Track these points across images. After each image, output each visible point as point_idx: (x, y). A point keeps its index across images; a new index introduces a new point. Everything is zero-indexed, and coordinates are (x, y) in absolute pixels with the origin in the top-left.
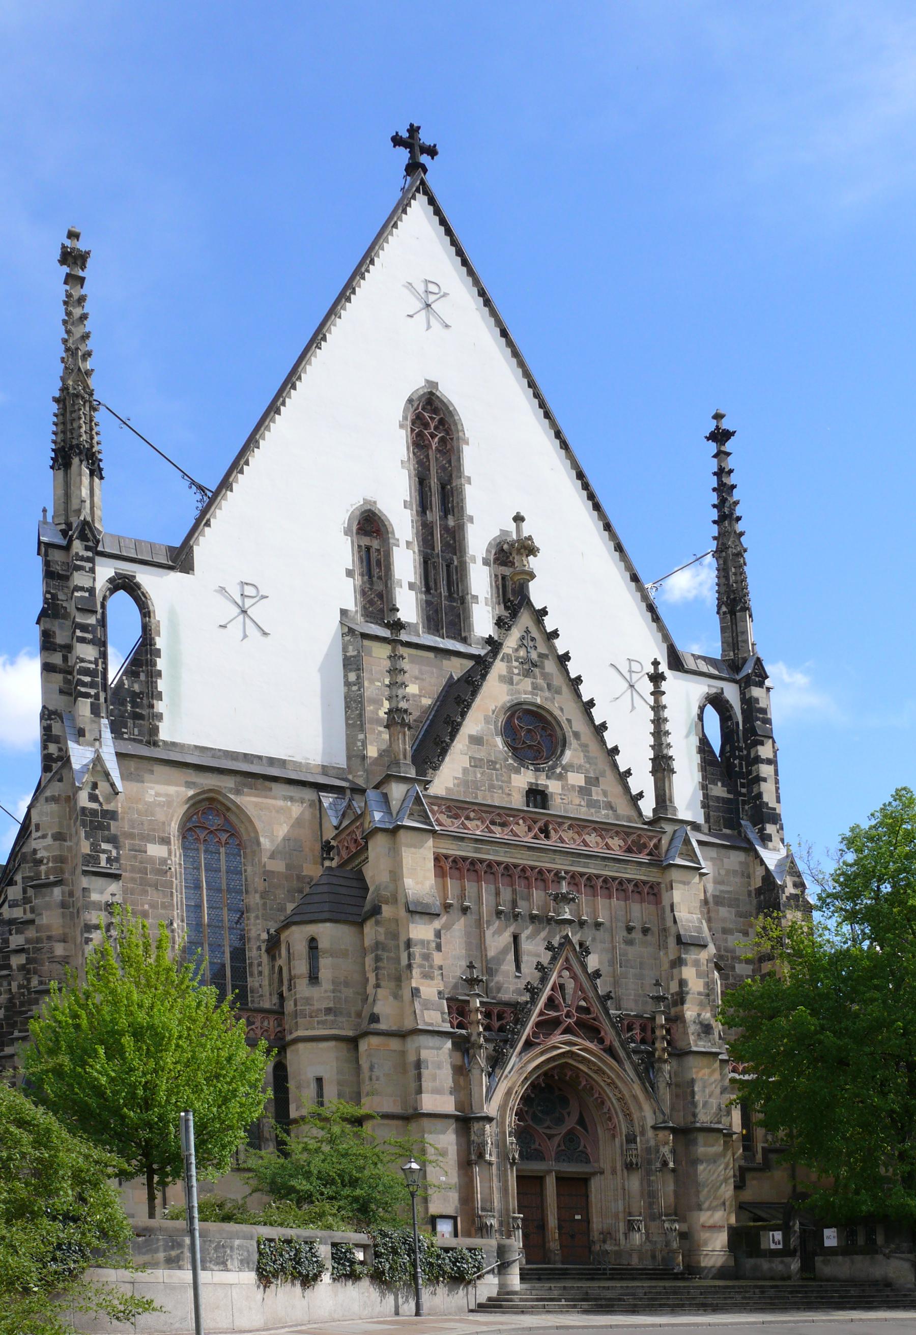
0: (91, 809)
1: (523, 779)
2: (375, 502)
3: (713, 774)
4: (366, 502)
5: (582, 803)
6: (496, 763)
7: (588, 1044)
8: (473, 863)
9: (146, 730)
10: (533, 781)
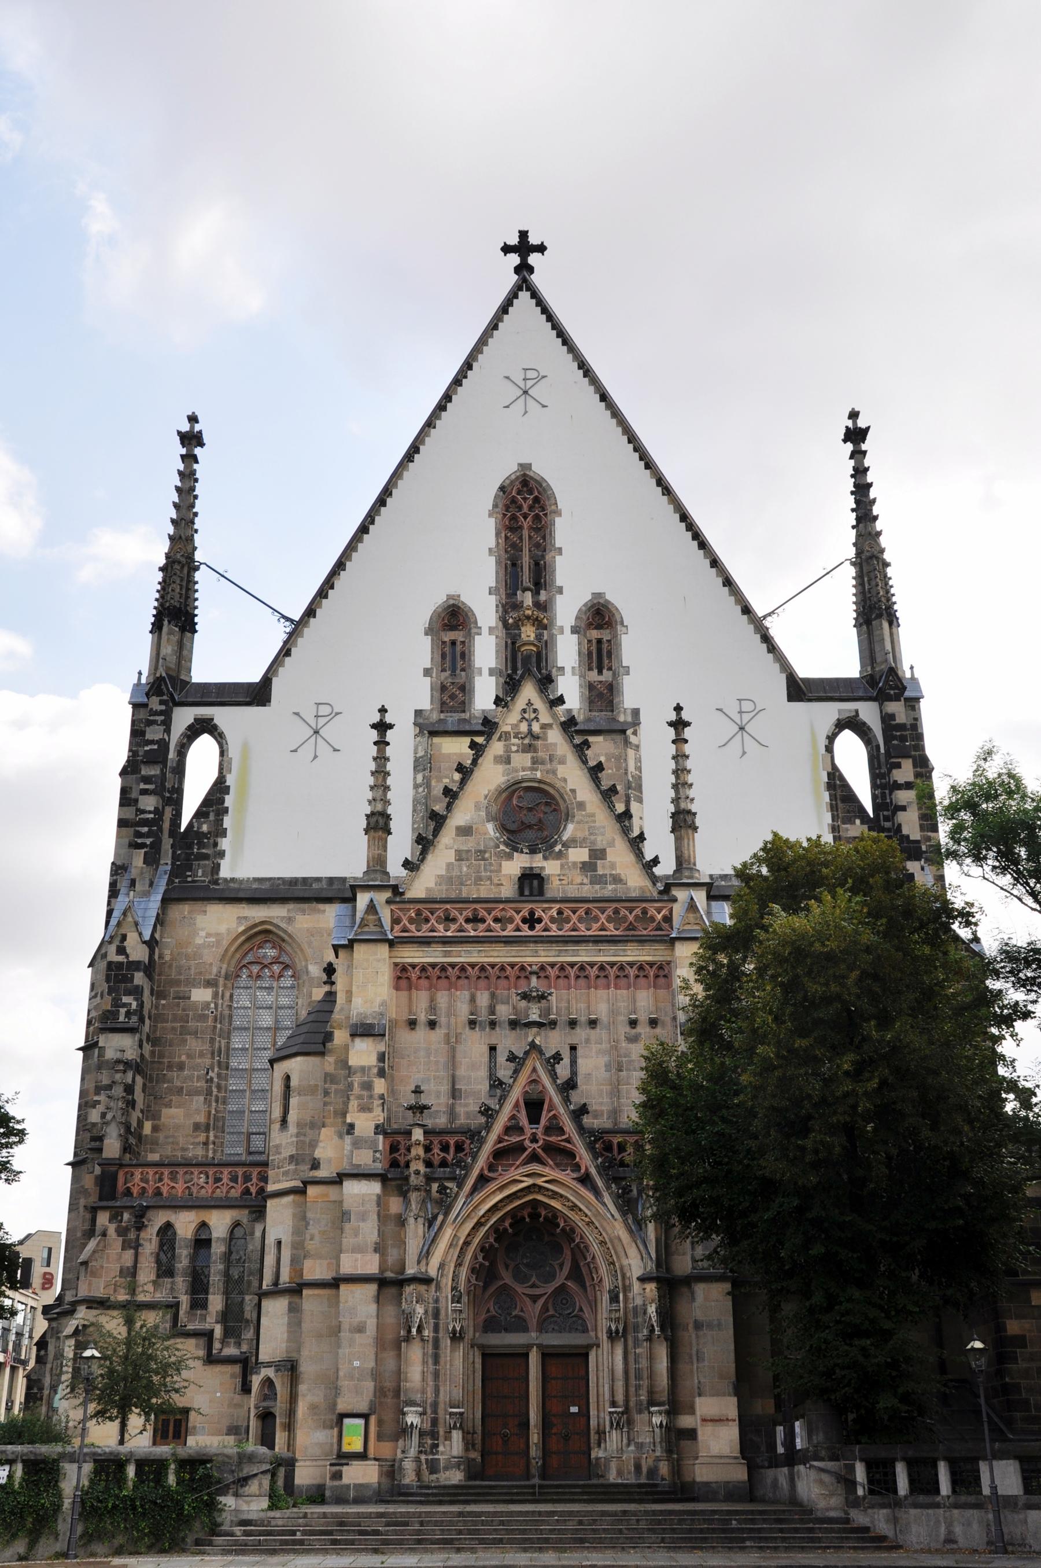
0: (118, 963)
1: (514, 866)
2: (459, 596)
3: (848, 812)
4: (449, 597)
5: (586, 881)
6: (485, 852)
7: (556, 1174)
8: (443, 969)
9: (209, 869)
10: (528, 865)
